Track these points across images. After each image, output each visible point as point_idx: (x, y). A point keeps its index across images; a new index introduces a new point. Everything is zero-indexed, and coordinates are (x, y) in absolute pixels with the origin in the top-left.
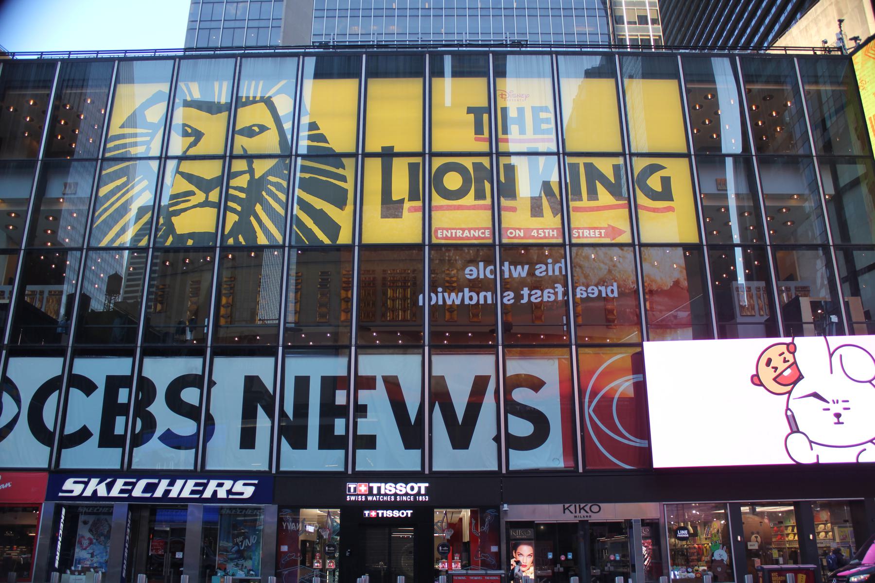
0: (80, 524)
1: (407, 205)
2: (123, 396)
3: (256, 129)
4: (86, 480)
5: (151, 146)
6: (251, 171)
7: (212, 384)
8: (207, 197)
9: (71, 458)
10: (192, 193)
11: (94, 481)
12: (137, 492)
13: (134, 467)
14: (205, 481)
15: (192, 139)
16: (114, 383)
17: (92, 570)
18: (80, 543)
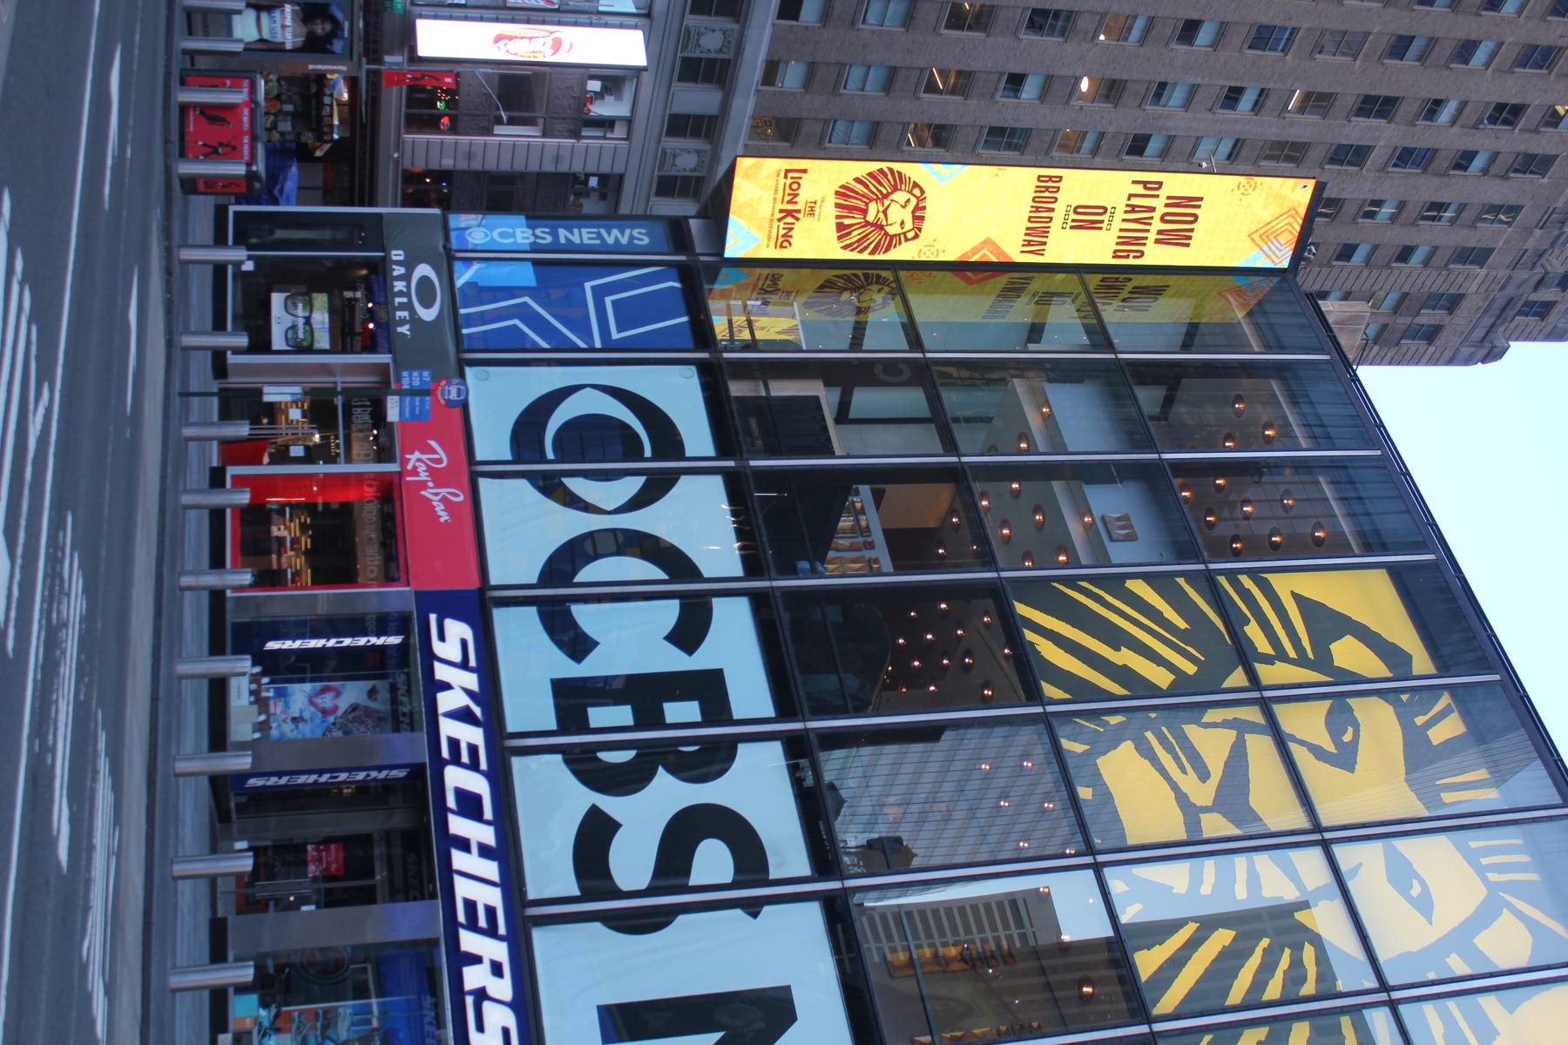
0: (366, 685)
2: (681, 711)
3: (1416, 891)
4: (473, 663)
5: (1279, 665)
7: (752, 907)
8: (1206, 810)
9: (519, 631)
10: (1204, 775)
11: (471, 681)
12: (455, 777)
13: (516, 762)
14: (502, 930)
15: (1330, 747)
16: (709, 689)
17: (262, 718)
18: (324, 690)
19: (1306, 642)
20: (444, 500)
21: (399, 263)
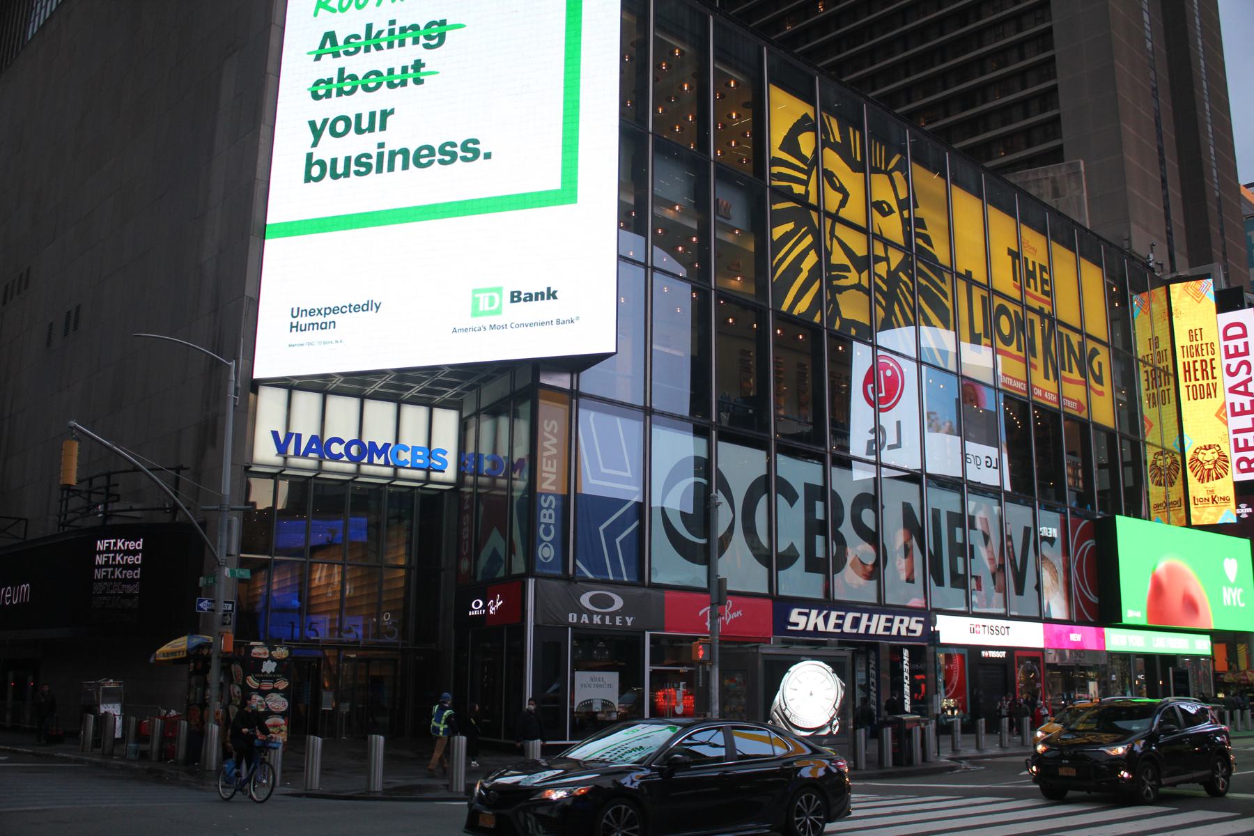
1: (984, 340)
6: (887, 259)
19: (802, 166)
20: (731, 612)
21: (579, 618)
